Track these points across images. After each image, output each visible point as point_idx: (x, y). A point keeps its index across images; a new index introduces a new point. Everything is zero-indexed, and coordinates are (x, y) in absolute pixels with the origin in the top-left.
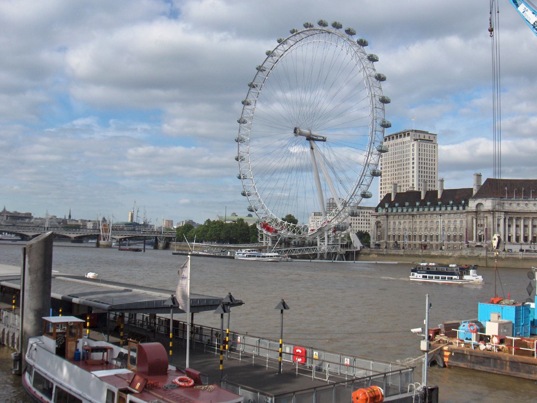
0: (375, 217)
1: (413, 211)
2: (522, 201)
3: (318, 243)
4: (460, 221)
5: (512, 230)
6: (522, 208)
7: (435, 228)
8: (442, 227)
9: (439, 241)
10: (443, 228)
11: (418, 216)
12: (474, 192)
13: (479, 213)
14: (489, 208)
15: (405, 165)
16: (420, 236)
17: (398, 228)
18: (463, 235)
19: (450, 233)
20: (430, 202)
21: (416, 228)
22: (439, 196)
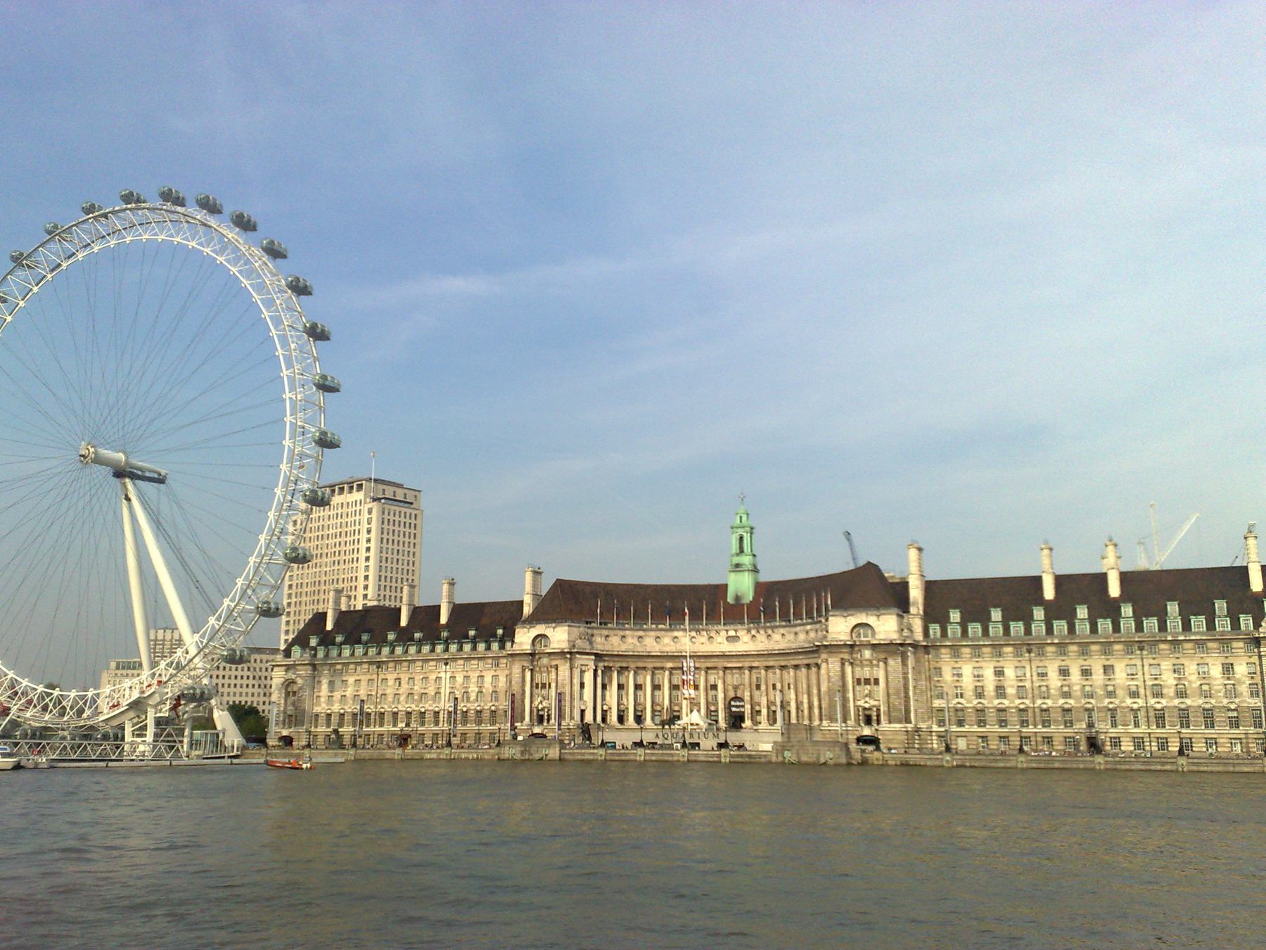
0: (284, 668)
1: (379, 653)
4: (493, 676)
5: (611, 696)
6: (631, 647)
7: (433, 694)
8: (448, 691)
9: (441, 725)
10: (450, 693)
11: (391, 665)
12: (527, 610)
13: (537, 657)
14: (563, 647)
15: (347, 552)
16: (395, 714)
18: (498, 709)
19: (469, 705)
20: (422, 632)
21: (385, 695)
22: (444, 619)
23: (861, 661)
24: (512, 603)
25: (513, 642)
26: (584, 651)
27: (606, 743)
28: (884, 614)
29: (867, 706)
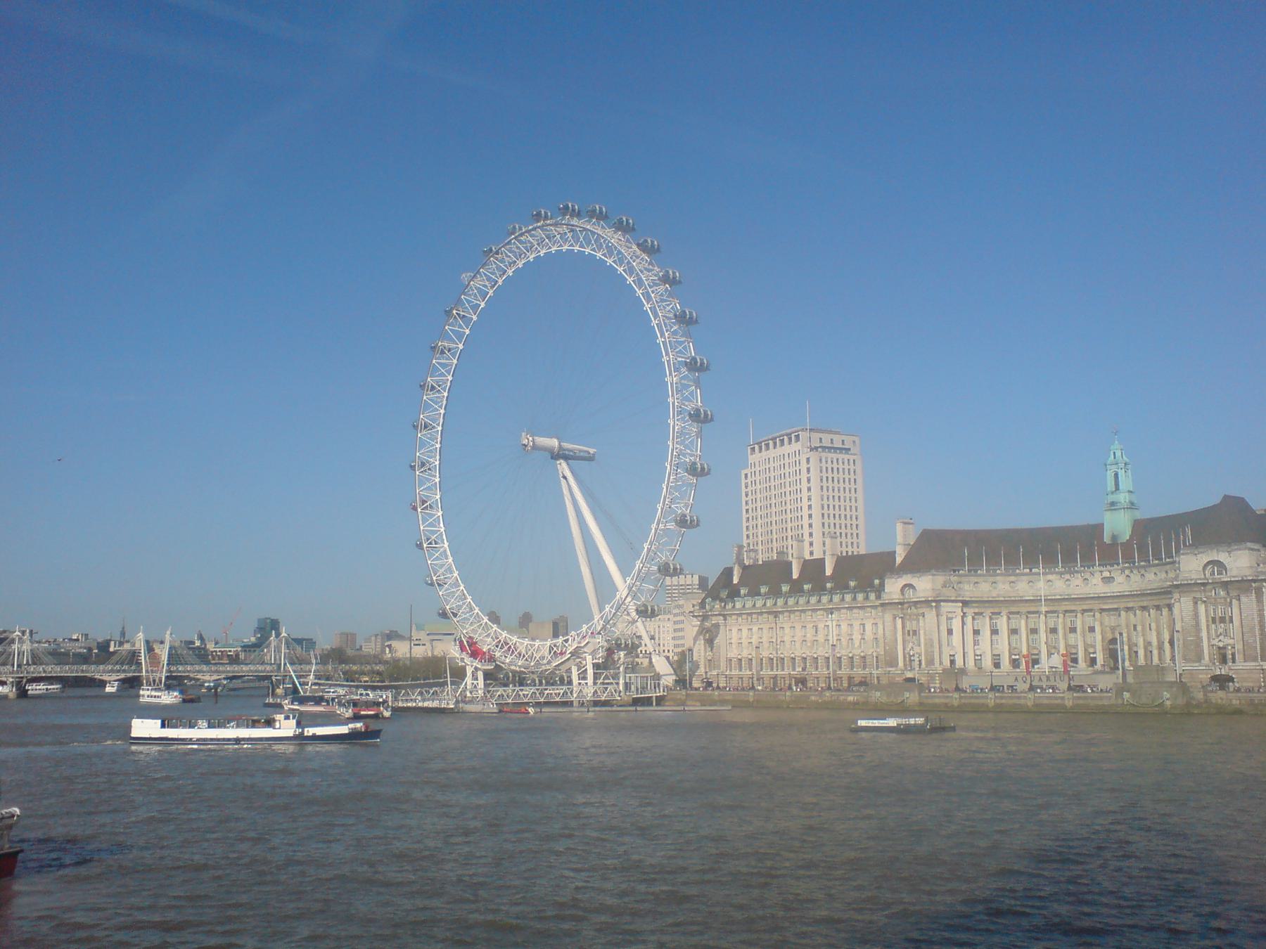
1: (775, 604)
2: (1001, 575)
3: (575, 681)
6: (1002, 593)
7: (823, 641)
8: (835, 638)
10: (837, 640)
12: (899, 560)
17: (747, 643)
20: (810, 583)
21: (783, 642)
22: (829, 572)
23: (1215, 599)
24: (888, 553)
25: (884, 590)
26: (949, 598)
27: (996, 686)
28: (1236, 549)
29: (1221, 645)
